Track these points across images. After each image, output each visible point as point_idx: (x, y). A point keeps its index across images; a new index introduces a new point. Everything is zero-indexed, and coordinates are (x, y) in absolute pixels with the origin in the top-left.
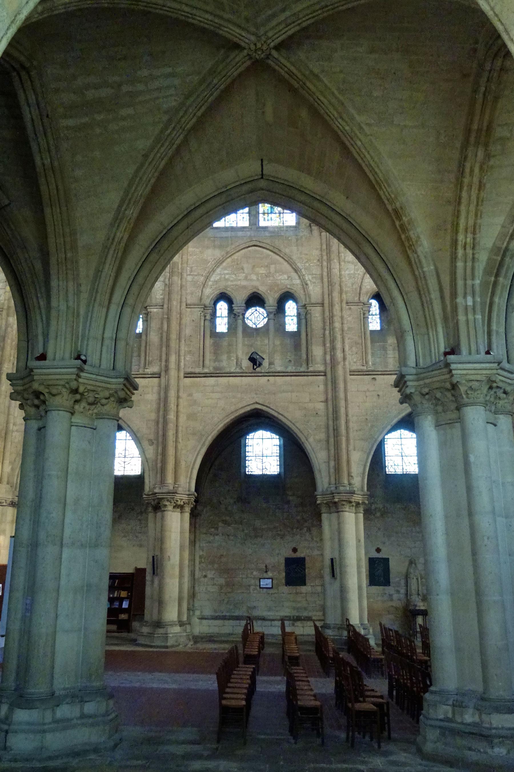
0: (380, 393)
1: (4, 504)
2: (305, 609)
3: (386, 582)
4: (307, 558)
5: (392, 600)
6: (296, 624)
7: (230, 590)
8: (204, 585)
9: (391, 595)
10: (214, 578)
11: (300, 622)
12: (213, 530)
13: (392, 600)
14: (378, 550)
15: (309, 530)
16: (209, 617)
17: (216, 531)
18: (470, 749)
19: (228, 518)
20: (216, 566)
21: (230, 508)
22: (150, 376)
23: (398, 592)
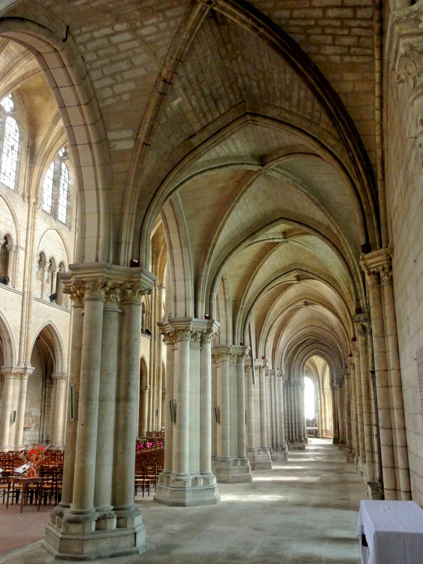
18: (205, 496)
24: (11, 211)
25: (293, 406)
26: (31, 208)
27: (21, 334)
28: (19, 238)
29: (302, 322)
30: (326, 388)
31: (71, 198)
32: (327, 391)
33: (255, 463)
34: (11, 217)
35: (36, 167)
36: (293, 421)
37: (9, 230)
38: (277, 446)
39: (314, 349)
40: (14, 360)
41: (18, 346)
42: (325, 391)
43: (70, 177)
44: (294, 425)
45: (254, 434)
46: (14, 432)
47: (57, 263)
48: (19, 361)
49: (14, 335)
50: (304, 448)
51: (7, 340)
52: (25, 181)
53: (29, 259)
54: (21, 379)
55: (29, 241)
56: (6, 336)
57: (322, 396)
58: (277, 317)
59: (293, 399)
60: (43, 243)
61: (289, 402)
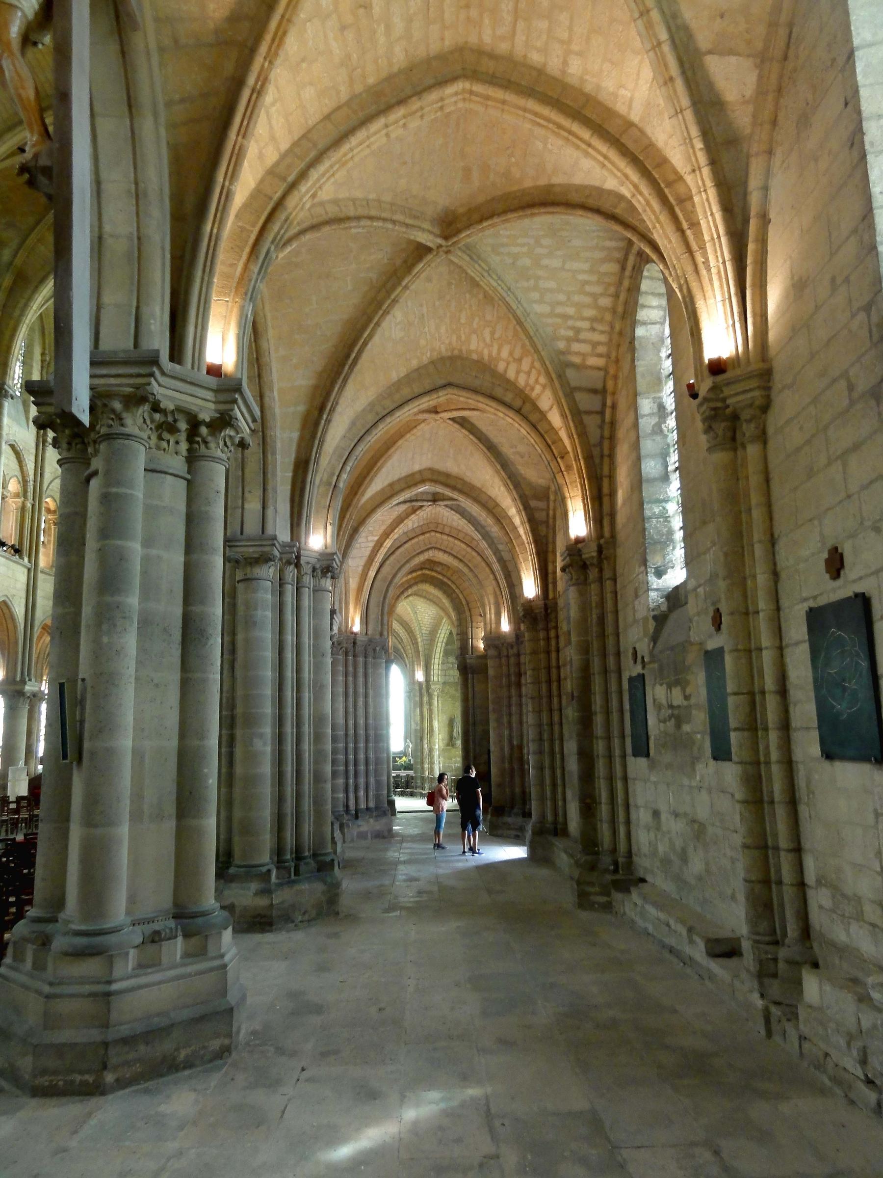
25: (361, 712)
29: (417, 370)
30: (436, 679)
32: (438, 687)
33: (106, 1045)
36: (362, 756)
38: (299, 857)
39: (427, 550)
42: (433, 687)
44: (362, 768)
45: (124, 830)
50: (390, 830)
57: (425, 699)
58: (312, 165)
59: (361, 690)
61: (351, 699)
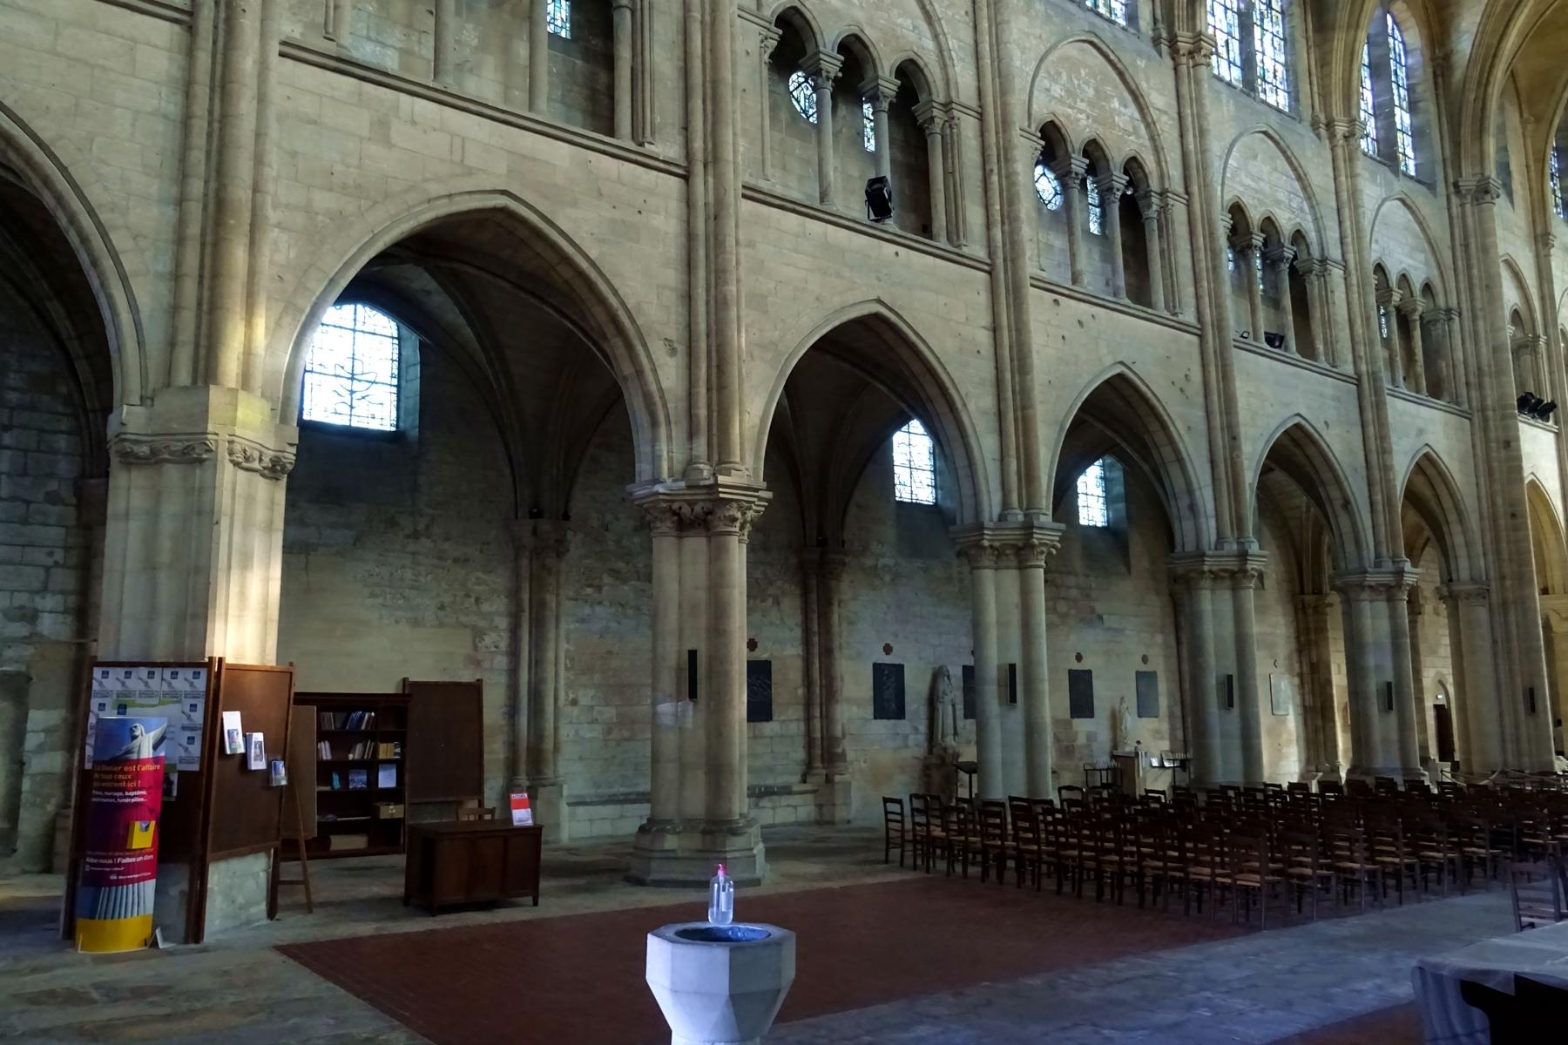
0: (1066, 335)
1: (256, 465)
2: (771, 770)
3: (900, 714)
4: (773, 663)
5: (907, 746)
6: (761, 804)
7: (626, 734)
8: (571, 722)
9: (906, 737)
10: (592, 707)
11: (767, 798)
12: (589, 590)
13: (907, 746)
14: (888, 649)
15: (777, 602)
16: (595, 799)
17: (596, 595)
19: (621, 565)
20: (597, 677)
21: (625, 542)
22: (662, 165)
23: (916, 730)
24: (1295, 170)
26: (1339, 151)
27: (1370, 485)
28: (1323, 236)
31: (1421, 105)
34: (1296, 185)
35: (1336, 37)
37: (1298, 220)
40: (1365, 553)
41: (1369, 515)
43: (1409, 48)
46: (1394, 736)
47: (1417, 286)
48: (1378, 556)
49: (1354, 489)
51: (1338, 504)
52: (1311, 83)
53: (1358, 287)
54: (1391, 600)
55: (1349, 240)
56: (1335, 493)
60: (1377, 241)
